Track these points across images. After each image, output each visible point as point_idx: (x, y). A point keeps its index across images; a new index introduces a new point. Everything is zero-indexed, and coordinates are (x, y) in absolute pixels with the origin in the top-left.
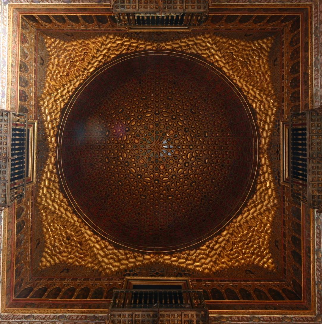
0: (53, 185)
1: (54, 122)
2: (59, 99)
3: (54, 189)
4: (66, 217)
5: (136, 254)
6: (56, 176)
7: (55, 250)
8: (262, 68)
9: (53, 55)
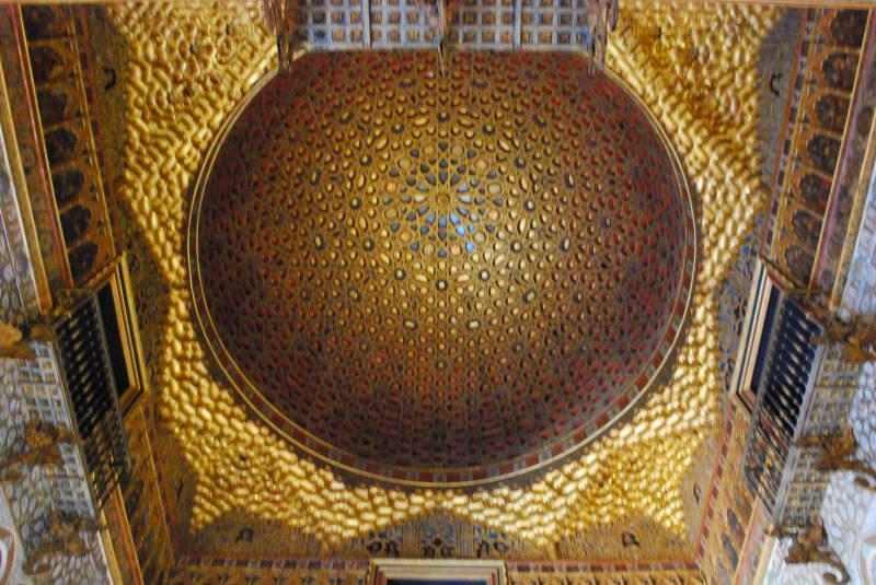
0: (193, 368)
1: (172, 224)
2: (173, 169)
3: (196, 377)
4: (233, 434)
5: (394, 495)
6: (197, 345)
7: (218, 486)
8: (737, 79)
9: (139, 37)
